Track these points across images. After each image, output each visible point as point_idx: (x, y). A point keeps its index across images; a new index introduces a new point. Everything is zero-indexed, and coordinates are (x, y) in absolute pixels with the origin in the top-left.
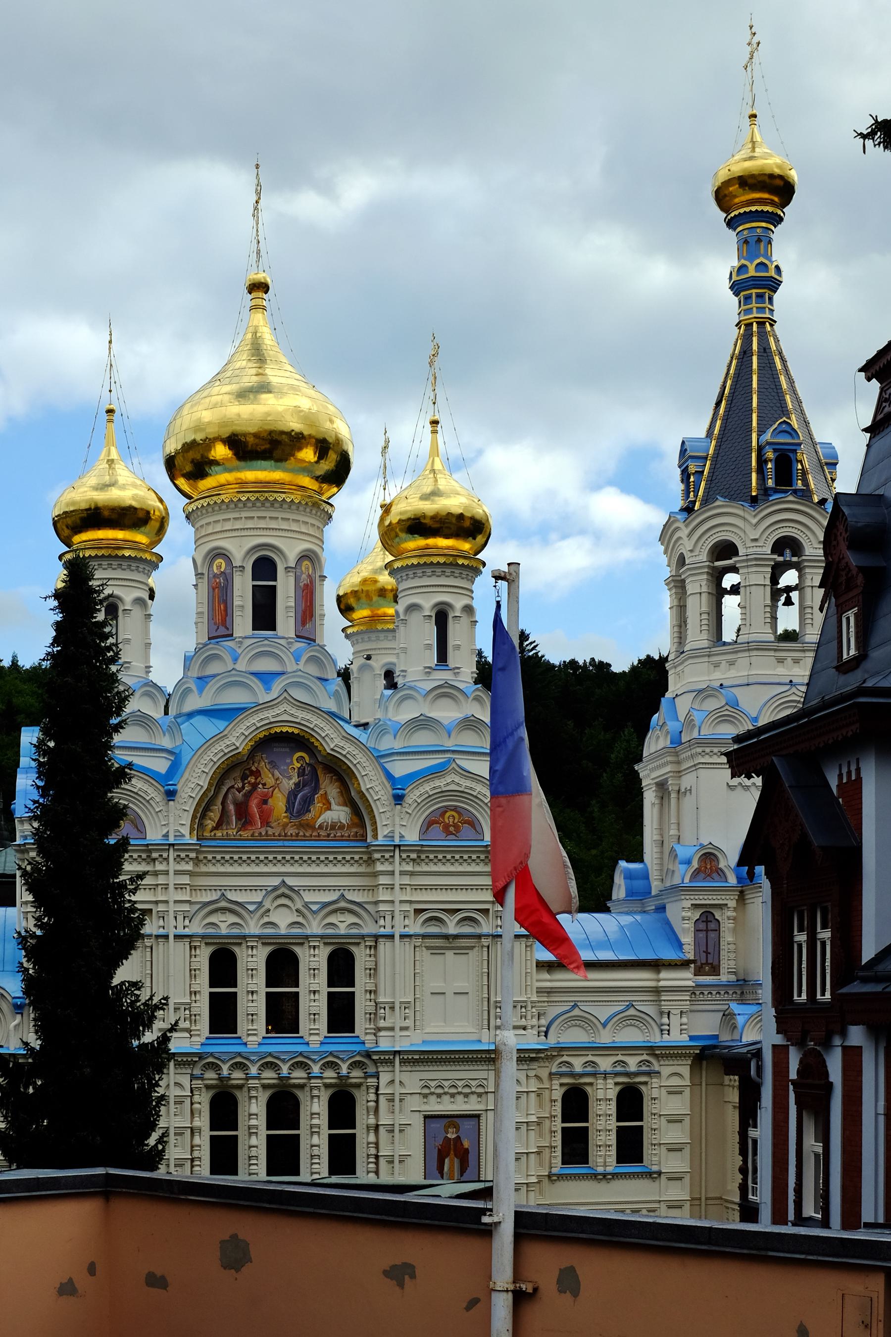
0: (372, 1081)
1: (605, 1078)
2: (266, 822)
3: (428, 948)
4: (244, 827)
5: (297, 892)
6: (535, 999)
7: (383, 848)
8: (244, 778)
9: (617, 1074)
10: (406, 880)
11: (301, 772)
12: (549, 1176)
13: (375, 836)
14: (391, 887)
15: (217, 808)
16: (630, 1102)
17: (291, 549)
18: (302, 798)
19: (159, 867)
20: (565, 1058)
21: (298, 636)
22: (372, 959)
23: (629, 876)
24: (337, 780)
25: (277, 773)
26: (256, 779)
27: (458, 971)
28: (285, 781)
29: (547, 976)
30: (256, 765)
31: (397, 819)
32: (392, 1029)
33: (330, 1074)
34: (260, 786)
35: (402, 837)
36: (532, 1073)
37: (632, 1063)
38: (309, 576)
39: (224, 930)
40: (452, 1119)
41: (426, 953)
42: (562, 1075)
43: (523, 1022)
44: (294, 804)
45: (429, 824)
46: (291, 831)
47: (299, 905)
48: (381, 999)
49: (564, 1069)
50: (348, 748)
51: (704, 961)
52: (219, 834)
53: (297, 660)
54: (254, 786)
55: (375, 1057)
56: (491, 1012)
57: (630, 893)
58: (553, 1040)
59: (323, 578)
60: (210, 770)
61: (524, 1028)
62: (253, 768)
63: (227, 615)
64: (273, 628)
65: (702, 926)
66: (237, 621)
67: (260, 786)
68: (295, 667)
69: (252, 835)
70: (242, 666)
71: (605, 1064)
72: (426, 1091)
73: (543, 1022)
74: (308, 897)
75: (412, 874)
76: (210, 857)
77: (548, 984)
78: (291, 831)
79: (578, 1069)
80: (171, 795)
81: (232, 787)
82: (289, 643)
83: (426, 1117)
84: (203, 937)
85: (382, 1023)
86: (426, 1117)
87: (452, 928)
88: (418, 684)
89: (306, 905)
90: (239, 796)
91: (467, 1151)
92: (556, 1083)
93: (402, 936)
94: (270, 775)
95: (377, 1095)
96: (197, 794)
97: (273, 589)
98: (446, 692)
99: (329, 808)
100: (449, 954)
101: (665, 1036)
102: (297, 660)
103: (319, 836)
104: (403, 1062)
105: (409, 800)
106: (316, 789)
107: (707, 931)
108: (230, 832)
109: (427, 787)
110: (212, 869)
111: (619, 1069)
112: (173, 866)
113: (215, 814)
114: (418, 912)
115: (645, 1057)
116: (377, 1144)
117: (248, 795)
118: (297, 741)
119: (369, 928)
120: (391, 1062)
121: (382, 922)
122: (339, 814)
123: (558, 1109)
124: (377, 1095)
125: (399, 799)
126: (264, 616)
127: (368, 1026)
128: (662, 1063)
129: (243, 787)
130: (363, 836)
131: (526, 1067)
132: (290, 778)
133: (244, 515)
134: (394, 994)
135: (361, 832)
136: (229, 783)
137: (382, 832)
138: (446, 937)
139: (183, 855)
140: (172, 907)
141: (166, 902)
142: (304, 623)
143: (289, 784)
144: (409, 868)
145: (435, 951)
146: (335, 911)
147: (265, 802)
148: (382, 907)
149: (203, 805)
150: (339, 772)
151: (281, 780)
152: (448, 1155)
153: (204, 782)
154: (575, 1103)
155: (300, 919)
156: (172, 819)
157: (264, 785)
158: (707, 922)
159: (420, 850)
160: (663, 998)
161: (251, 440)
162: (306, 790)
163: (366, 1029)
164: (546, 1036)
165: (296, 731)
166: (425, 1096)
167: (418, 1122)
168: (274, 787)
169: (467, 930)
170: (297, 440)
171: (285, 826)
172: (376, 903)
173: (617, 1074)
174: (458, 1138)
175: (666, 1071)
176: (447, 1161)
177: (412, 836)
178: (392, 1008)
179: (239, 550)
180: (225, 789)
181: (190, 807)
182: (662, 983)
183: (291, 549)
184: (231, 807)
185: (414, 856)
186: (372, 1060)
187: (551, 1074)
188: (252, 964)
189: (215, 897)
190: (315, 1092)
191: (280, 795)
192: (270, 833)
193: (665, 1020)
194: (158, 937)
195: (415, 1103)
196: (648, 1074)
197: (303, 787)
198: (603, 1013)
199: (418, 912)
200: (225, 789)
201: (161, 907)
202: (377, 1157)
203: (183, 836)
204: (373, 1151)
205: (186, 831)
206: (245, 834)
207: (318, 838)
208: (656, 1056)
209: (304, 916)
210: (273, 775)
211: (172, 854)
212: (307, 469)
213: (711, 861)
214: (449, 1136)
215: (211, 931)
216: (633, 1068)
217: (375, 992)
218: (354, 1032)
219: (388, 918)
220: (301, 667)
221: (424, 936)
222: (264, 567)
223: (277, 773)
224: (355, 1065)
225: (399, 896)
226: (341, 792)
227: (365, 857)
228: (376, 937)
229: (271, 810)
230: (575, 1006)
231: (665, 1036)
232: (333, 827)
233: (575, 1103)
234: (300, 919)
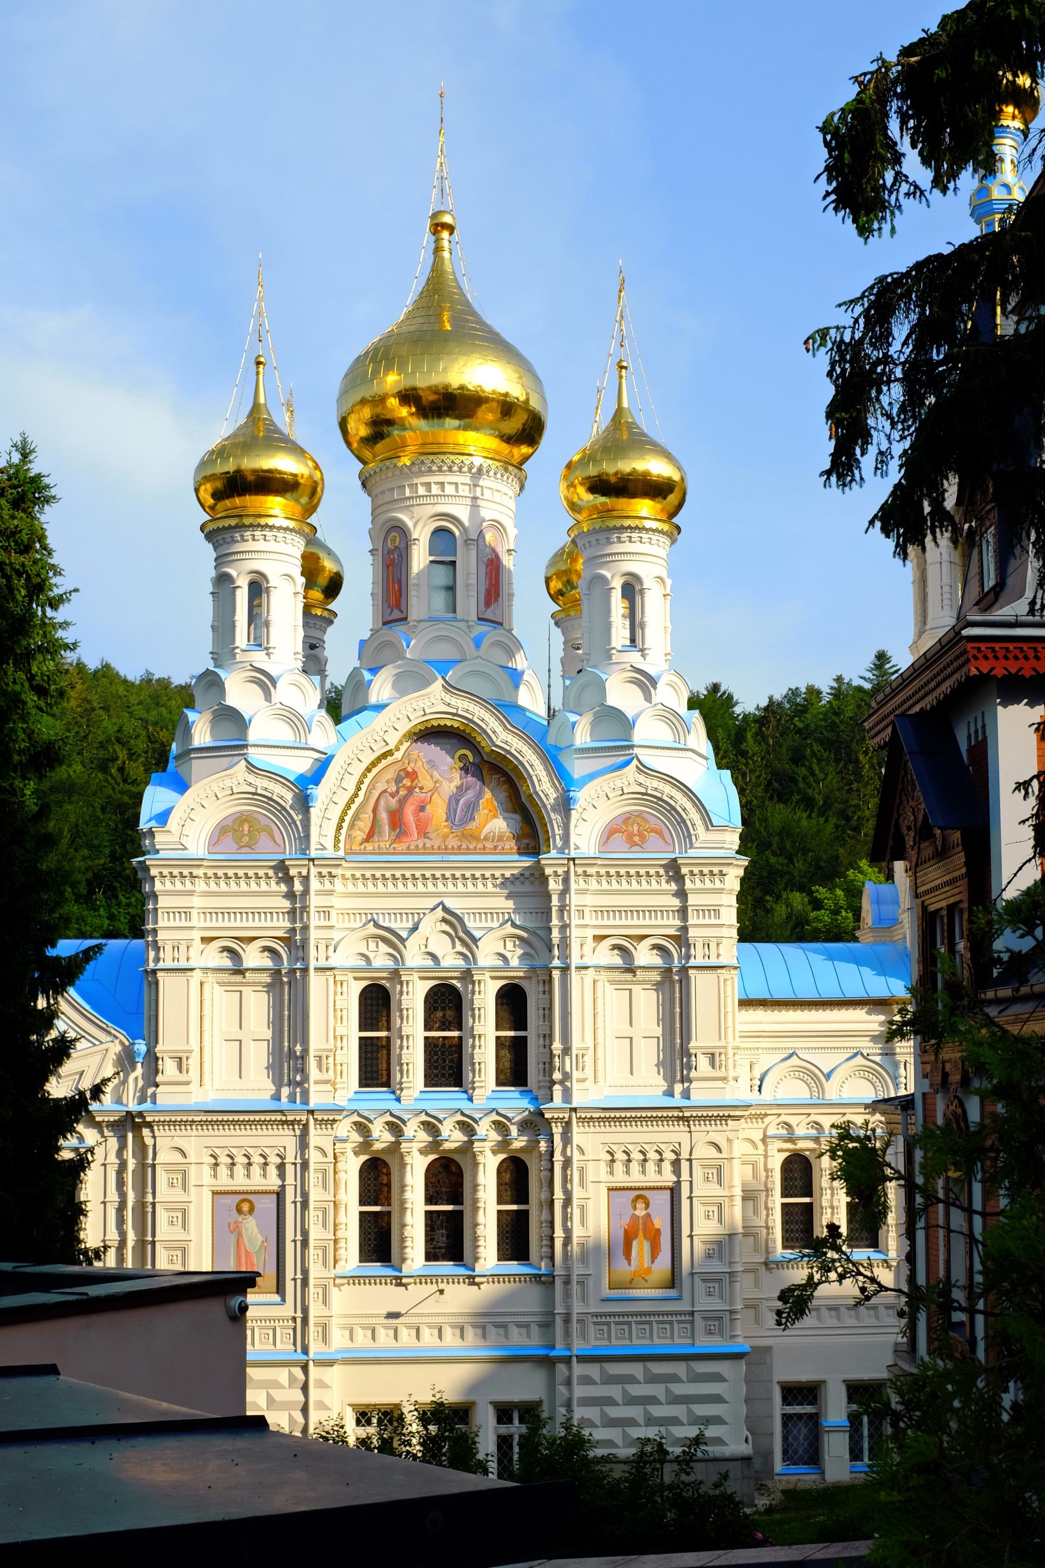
2: (423, 833)
4: (398, 839)
12: (766, 1264)
15: (367, 816)
18: (464, 804)
21: (479, 619)
22: (547, 996)
23: (878, 901)
24: (505, 782)
25: (435, 773)
26: (412, 782)
28: (445, 784)
30: (412, 765)
34: (417, 790)
44: (455, 810)
46: (452, 842)
52: (369, 847)
53: (478, 646)
54: (410, 790)
57: (879, 919)
58: (767, 1096)
62: (409, 769)
63: (401, 596)
67: (417, 790)
68: (476, 653)
69: (408, 848)
73: (757, 1075)
78: (452, 842)
81: (385, 791)
90: (393, 802)
91: (658, 1232)
94: (429, 777)
102: (478, 646)
103: (484, 848)
108: (382, 845)
113: (365, 824)
114: (599, 938)
117: (402, 802)
127: (541, 1078)
129: (397, 792)
130: (535, 848)
132: (451, 780)
135: (532, 844)
142: (488, 604)
147: (422, 809)
149: (350, 813)
152: (636, 1236)
157: (421, 788)
163: (539, 1082)
164: (760, 1091)
165: (456, 725)
171: (445, 837)
174: (648, 1215)
176: (635, 1244)
184: (384, 816)
188: (413, 1000)
191: (439, 801)
192: (428, 845)
197: (467, 790)
199: (599, 938)
206: (400, 847)
207: (484, 851)
210: (432, 777)
214: (637, 1213)
218: (526, 1085)
223: (435, 773)
226: (510, 797)
227: (537, 874)
229: (429, 819)
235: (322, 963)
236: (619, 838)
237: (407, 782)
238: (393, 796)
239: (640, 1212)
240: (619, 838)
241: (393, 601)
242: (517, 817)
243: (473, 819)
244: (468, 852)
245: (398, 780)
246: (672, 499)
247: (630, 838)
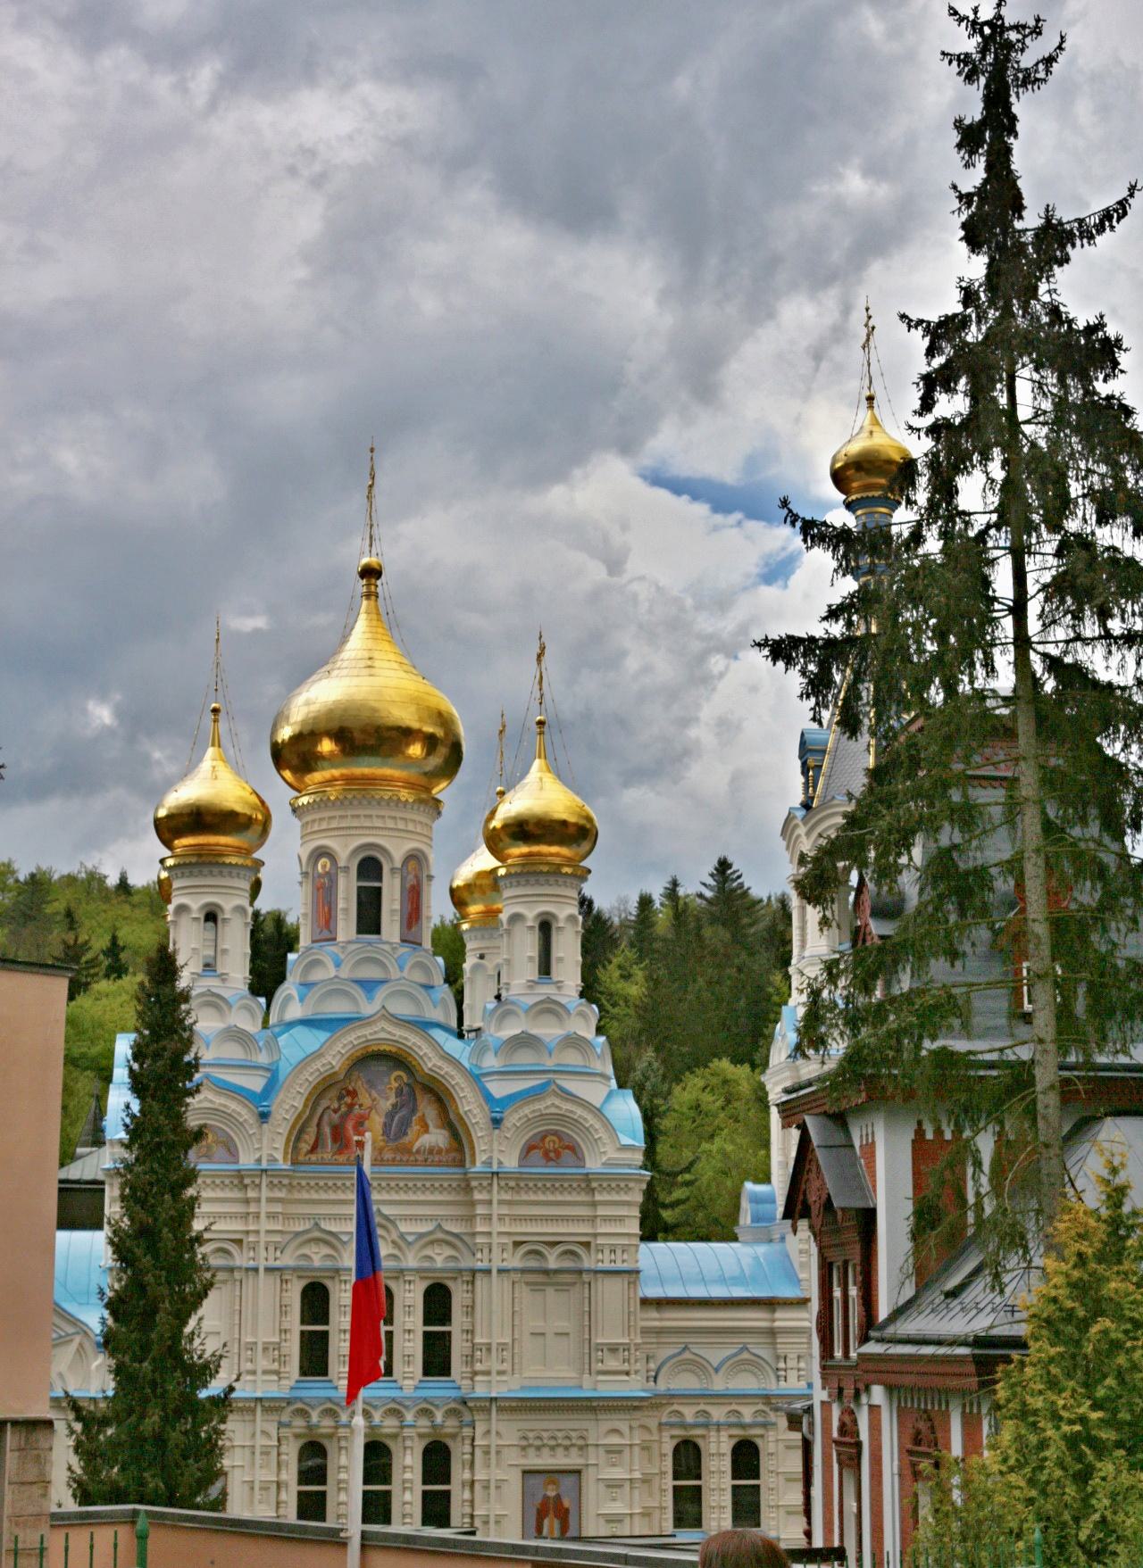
0: (467, 1431)
1: (718, 1431)
3: (527, 1284)
4: (340, 1152)
5: (393, 1222)
6: (639, 1341)
7: (480, 1176)
8: (340, 1098)
9: (730, 1425)
10: (505, 1210)
11: (399, 1092)
13: (473, 1162)
14: (488, 1218)
15: (312, 1130)
16: (746, 1458)
17: (397, 850)
19: (251, 1194)
20: (675, 1407)
21: (403, 941)
25: (375, 1094)
27: (556, 1310)
29: (655, 1315)
31: (495, 1146)
32: (488, 1373)
33: (424, 1422)
35: (500, 1163)
36: (635, 1424)
38: (416, 876)
39: (317, 1263)
40: (553, 1474)
41: (525, 1289)
42: (672, 1425)
43: (626, 1367)
45: (529, 1149)
46: (388, 1155)
47: (395, 1236)
48: (478, 1340)
49: (674, 1419)
50: (447, 1068)
52: (313, 1158)
53: (401, 969)
54: (351, 1106)
55: (471, 1404)
56: (590, 1354)
58: (662, 1386)
59: (430, 878)
60: (305, 1090)
61: (627, 1373)
64: (377, 931)
66: (341, 925)
68: (399, 975)
70: (345, 973)
71: (718, 1413)
72: (524, 1443)
73: (652, 1366)
74: (403, 1227)
75: (510, 1203)
76: (304, 1183)
77: (657, 1324)
78: (388, 1155)
79: (689, 1419)
80: (264, 1117)
82: (394, 949)
83: (524, 1472)
84: (294, 1269)
85: (478, 1367)
86: (524, 1472)
87: (553, 1262)
88: (522, 999)
89: (402, 1236)
90: (336, 1117)
91: (567, 1511)
92: (666, 1434)
93: (500, 1271)
95: (473, 1446)
96: (291, 1117)
97: (379, 890)
98: (550, 1009)
99: (427, 1131)
100: (550, 1291)
101: (782, 1383)
102: (401, 969)
104: (500, 1410)
105: (507, 1123)
106: (414, 1111)
109: (527, 1110)
110: (305, 1196)
111: (733, 1419)
112: (265, 1193)
113: (310, 1137)
114: (517, 1244)
115: (761, 1407)
116: (472, 1502)
117: (344, 1117)
118: (397, 1060)
119: (467, 1262)
120: (489, 1411)
121: (479, 1255)
122: (436, 1137)
123: (668, 1464)
124: (473, 1446)
125: (497, 1122)
126: (369, 921)
133: (349, 813)
134: (490, 1336)
136: (324, 1103)
137: (481, 1158)
138: (546, 1272)
139: (276, 1181)
140: (263, 1238)
141: (257, 1232)
142: (409, 926)
143: (386, 1105)
145: (535, 1287)
146: (432, 1242)
148: (479, 1240)
150: (439, 1095)
151: (379, 1099)
153: (299, 1103)
154: (688, 1458)
155: (396, 1252)
156: (265, 1142)
159: (518, 1177)
161: (356, 734)
162: (404, 1112)
166: (524, 1448)
167: (515, 1479)
168: (370, 1109)
169: (568, 1264)
170: (407, 734)
172: (474, 1234)
173: (730, 1425)
174: (558, 1497)
176: (546, 1522)
177: (511, 1162)
178: (489, 1350)
179: (344, 849)
180: (320, 1110)
181: (284, 1129)
182: (777, 1324)
183: (397, 850)
184: (327, 1130)
185: (512, 1184)
186: (464, 1407)
187: (660, 1424)
189: (308, 1226)
190: (408, 1443)
193: (782, 1365)
194: (247, 1270)
195: (513, 1457)
196: (765, 1425)
198: (715, 1356)
199: (517, 1244)
200: (320, 1110)
201: (252, 1238)
202: (472, 1516)
203: (276, 1160)
204: (468, 1510)
205: (279, 1156)
206: (341, 1158)
209: (400, 1249)
211: (265, 1181)
212: (412, 762)
215: (303, 1263)
216: (748, 1419)
217: (473, 1332)
219: (486, 1251)
220: (405, 974)
221: (524, 1271)
222: (370, 867)
224: (452, 1413)
225: (497, 1227)
228: (474, 1272)
230: (686, 1348)
231: (782, 1383)
232: (431, 1151)
233: (688, 1458)
234: (396, 1252)
235: (271, 1263)
236: (537, 1155)
237: (348, 1100)
238: (335, 1111)
239: (551, 1493)
240: (537, 1155)
241: (322, 922)
242: (445, 1133)
243: (405, 1134)
244: (401, 1163)
245: (340, 1098)
246: (585, 846)
247: (546, 1155)
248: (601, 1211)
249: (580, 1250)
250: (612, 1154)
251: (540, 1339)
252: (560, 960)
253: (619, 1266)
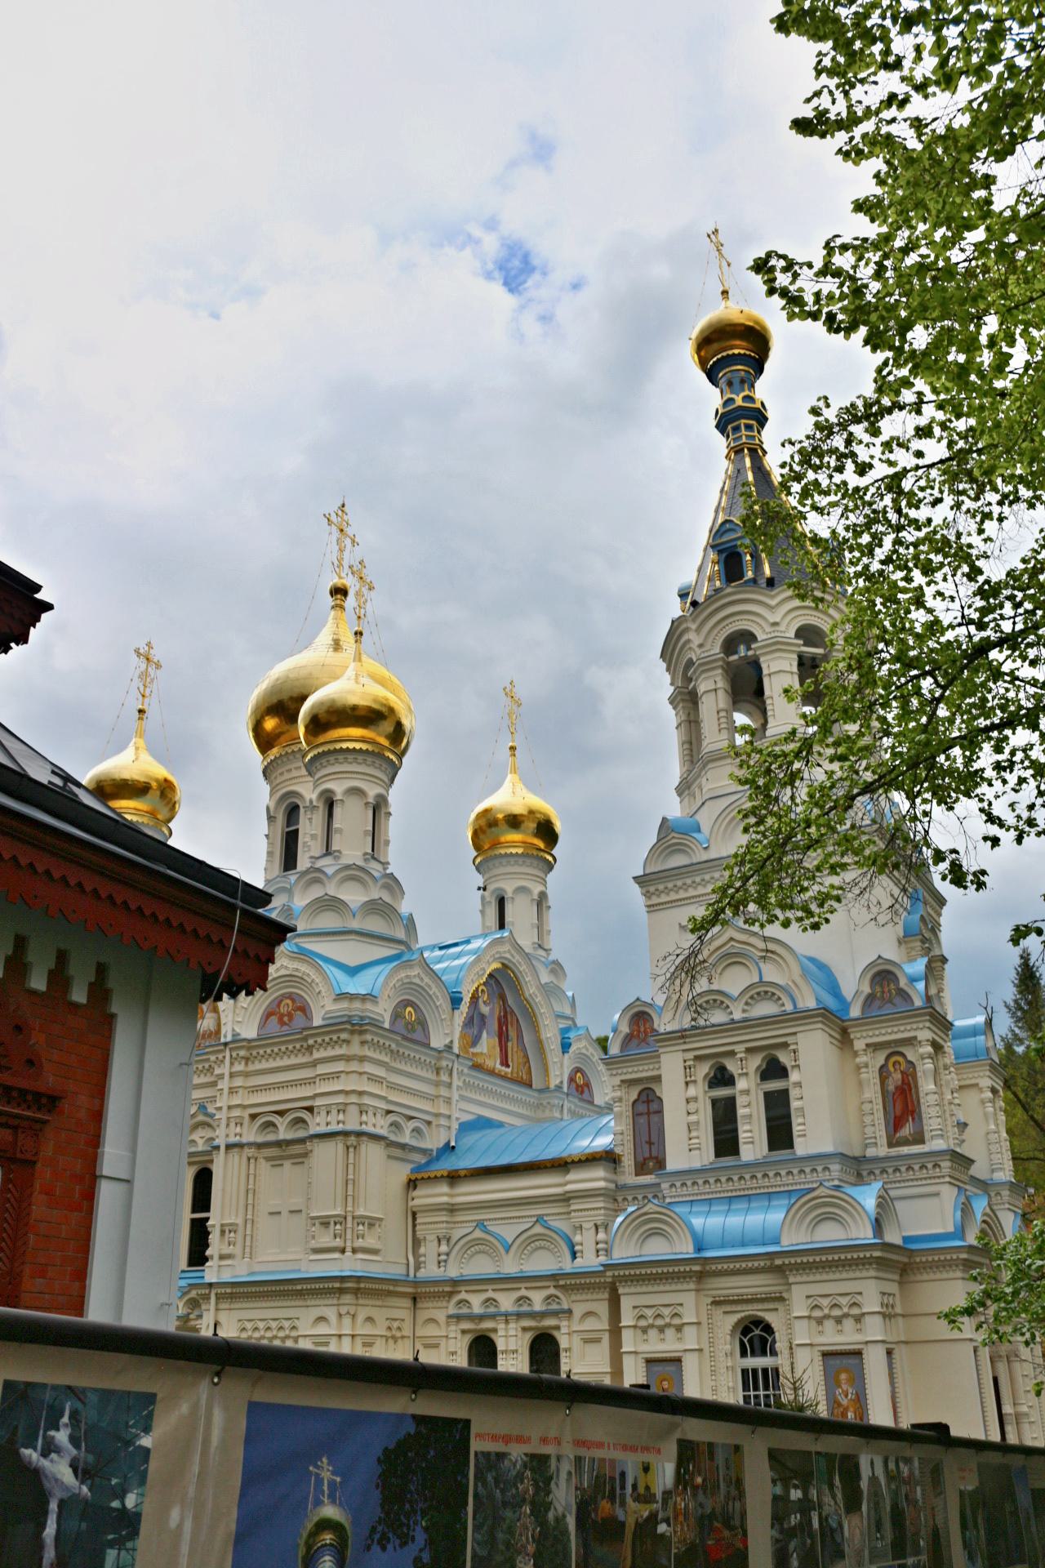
1: (507, 1322)
3: (267, 1159)
9: (519, 1316)
37: (538, 1300)
41: (262, 1163)
42: (459, 1318)
43: (338, 1242)
51: (647, 1155)
61: (343, 1251)
65: (642, 1108)
87: (284, 1133)
100: (287, 1164)
107: (648, 1113)
115: (552, 1291)
128: (574, 1297)
131: (335, 1302)
138: (278, 1144)
144: (239, 1067)
145: (276, 1162)
158: (648, 1102)
160: (573, 1207)
175: (578, 1310)
196: (555, 1314)
199: (253, 1117)
208: (563, 1288)
213: (645, 1021)
236: (274, 1019)
240: (274, 1019)
247: (281, 1017)
248: (322, 1069)
249: (305, 1115)
250: (331, 1006)
251: (276, 1217)
252: (340, 831)
253: (334, 1128)
